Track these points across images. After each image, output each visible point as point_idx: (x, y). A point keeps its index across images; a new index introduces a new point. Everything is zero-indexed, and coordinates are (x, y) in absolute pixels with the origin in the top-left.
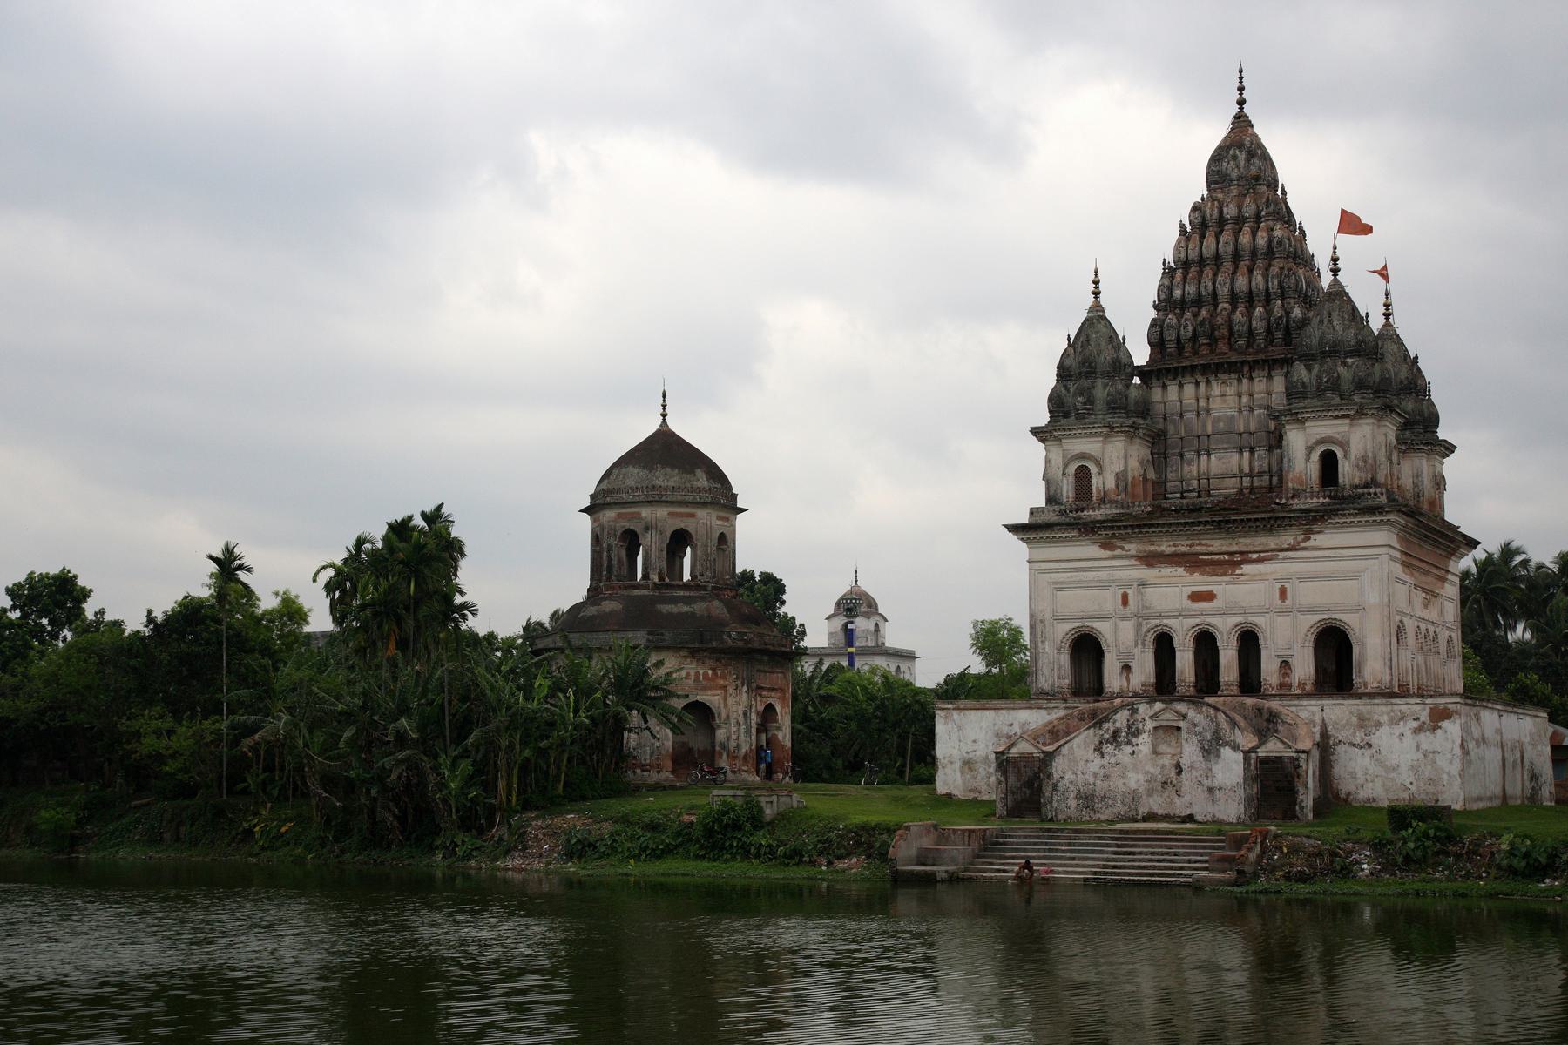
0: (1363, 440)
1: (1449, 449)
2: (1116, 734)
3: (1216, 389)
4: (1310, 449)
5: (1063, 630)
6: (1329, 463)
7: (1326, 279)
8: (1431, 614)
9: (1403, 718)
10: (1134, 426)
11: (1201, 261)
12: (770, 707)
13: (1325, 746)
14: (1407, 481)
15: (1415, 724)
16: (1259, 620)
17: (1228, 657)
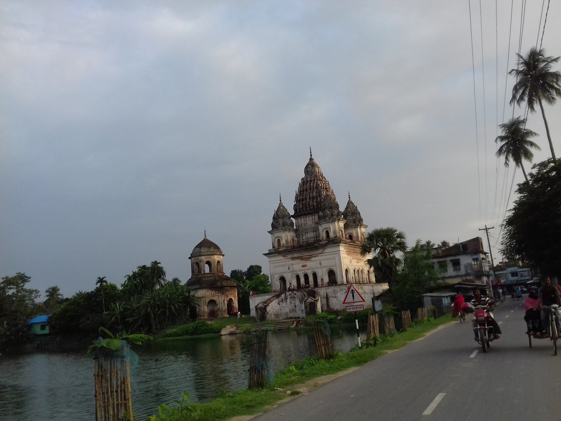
3: (308, 219)
6: (327, 233)
9: (342, 290)
12: (231, 299)
13: (327, 298)
14: (354, 234)
15: (344, 291)
16: (316, 270)
17: (311, 279)
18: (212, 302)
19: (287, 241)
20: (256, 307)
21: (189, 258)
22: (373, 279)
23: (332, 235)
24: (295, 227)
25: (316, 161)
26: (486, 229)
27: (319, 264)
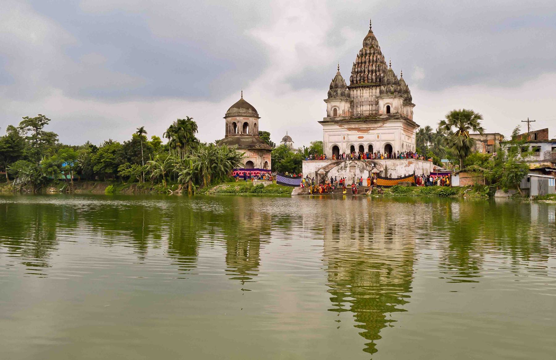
0: (396, 103)
1: (414, 105)
2: (342, 167)
4: (384, 105)
6: (388, 108)
7: (388, 68)
8: (409, 141)
9: (402, 164)
10: (347, 100)
11: (362, 63)
12: (266, 162)
13: (386, 170)
14: (405, 113)
17: (366, 150)
18: (250, 163)
19: (343, 111)
20: (316, 172)
23: (392, 110)
25: (375, 34)
26: (528, 121)
27: (376, 137)
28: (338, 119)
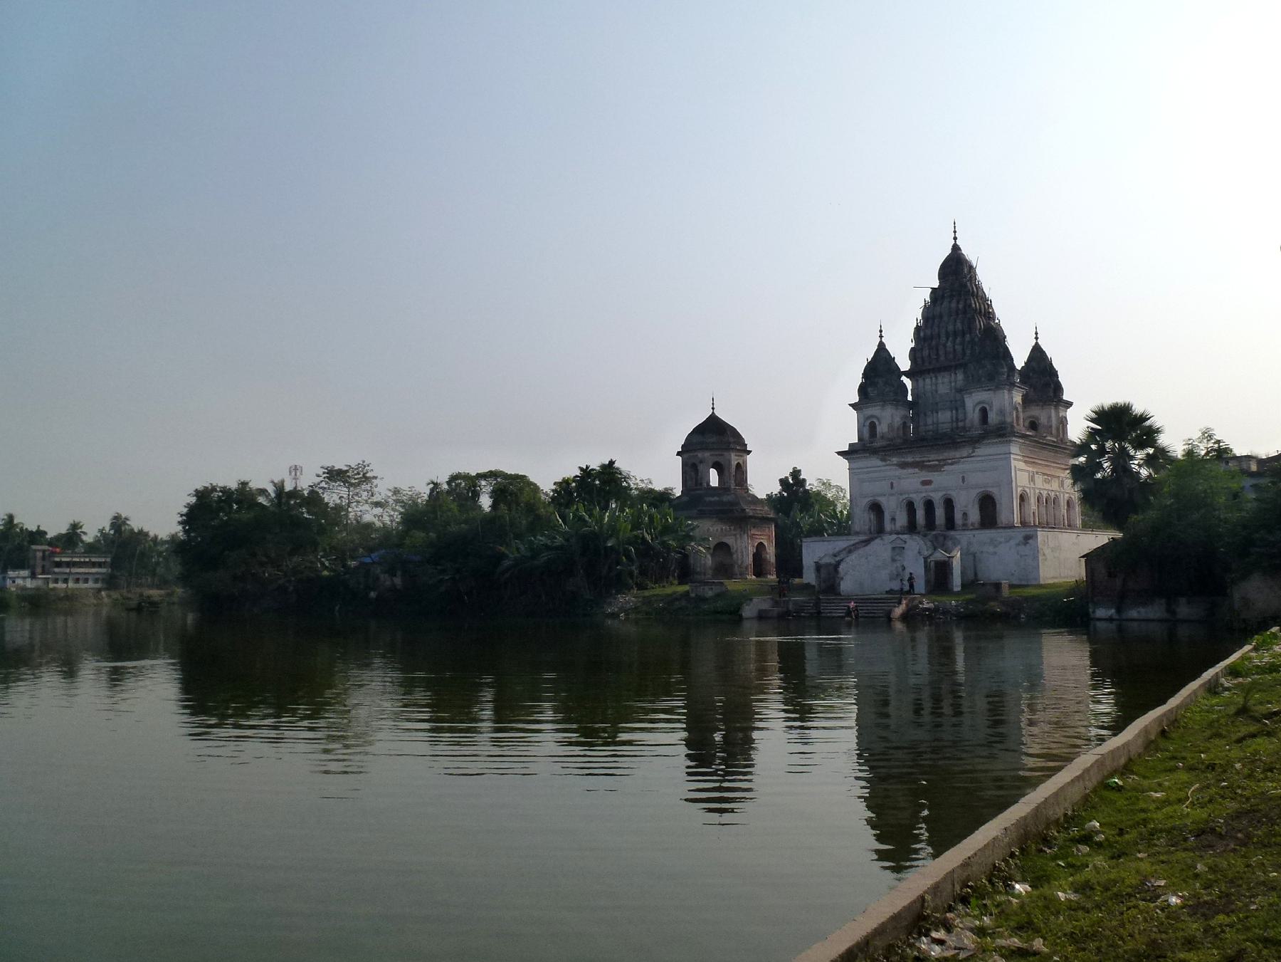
1: (1069, 404)
3: (940, 381)
5: (865, 502)
6: (984, 412)
17: (940, 513)
18: (722, 548)
19: (890, 426)
21: (679, 454)
22: (1078, 522)
23: (993, 417)
24: (910, 398)
28: (877, 444)
